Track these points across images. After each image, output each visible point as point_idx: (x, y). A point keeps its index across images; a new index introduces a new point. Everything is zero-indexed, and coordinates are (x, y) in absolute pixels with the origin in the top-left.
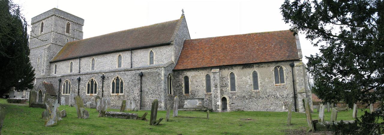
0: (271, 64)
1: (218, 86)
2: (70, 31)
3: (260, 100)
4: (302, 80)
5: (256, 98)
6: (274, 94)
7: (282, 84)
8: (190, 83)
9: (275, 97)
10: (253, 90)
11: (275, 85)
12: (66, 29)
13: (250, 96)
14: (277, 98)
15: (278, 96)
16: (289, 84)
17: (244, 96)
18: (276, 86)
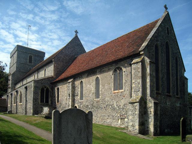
0: (111, 66)
1: (71, 95)
2: (33, 61)
3: (100, 111)
4: (139, 84)
5: (97, 108)
6: (111, 103)
7: (121, 91)
8: (60, 93)
9: (112, 107)
10: (95, 99)
11: (113, 92)
12: (28, 60)
13: (92, 105)
14: (114, 109)
15: (115, 106)
16: (128, 90)
17: (87, 106)
18: (114, 93)
